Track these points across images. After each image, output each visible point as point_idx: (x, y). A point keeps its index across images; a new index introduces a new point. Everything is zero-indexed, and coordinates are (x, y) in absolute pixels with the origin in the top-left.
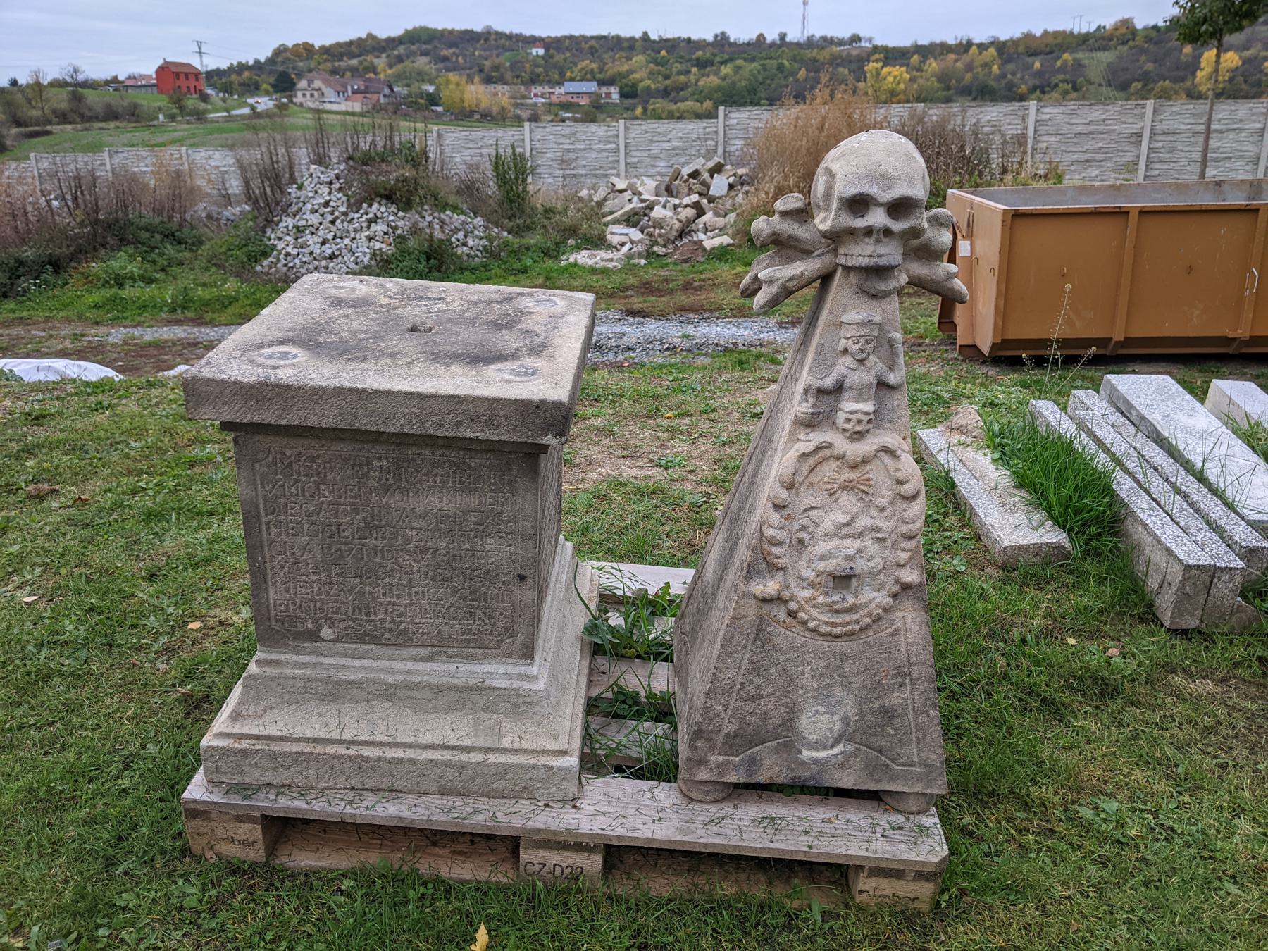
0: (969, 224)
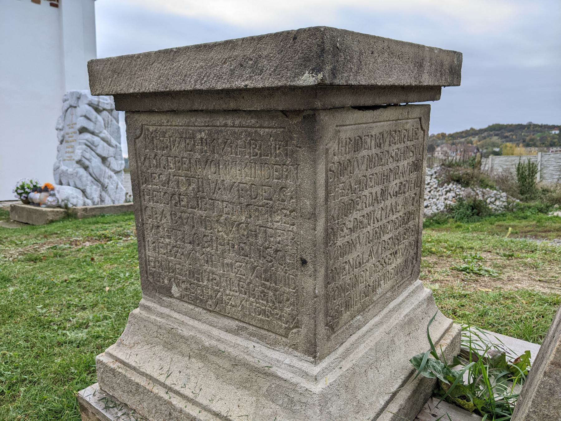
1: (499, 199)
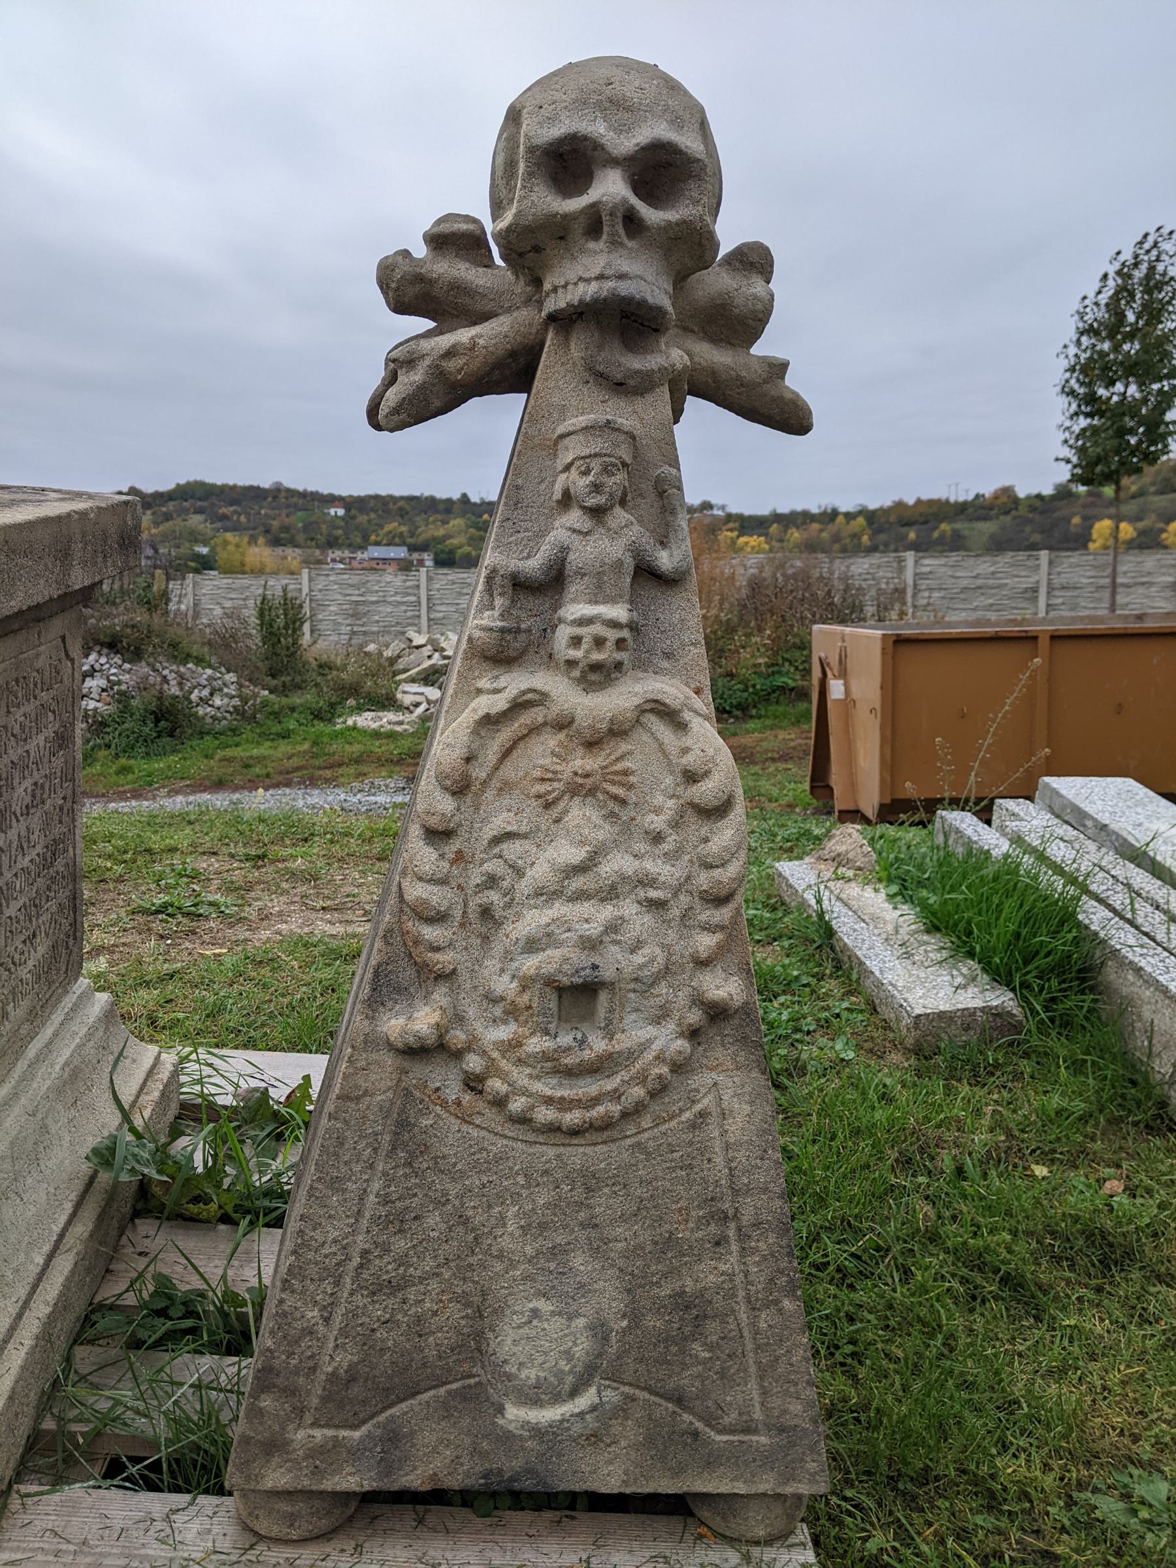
0: (842, 661)
1: (220, 690)
